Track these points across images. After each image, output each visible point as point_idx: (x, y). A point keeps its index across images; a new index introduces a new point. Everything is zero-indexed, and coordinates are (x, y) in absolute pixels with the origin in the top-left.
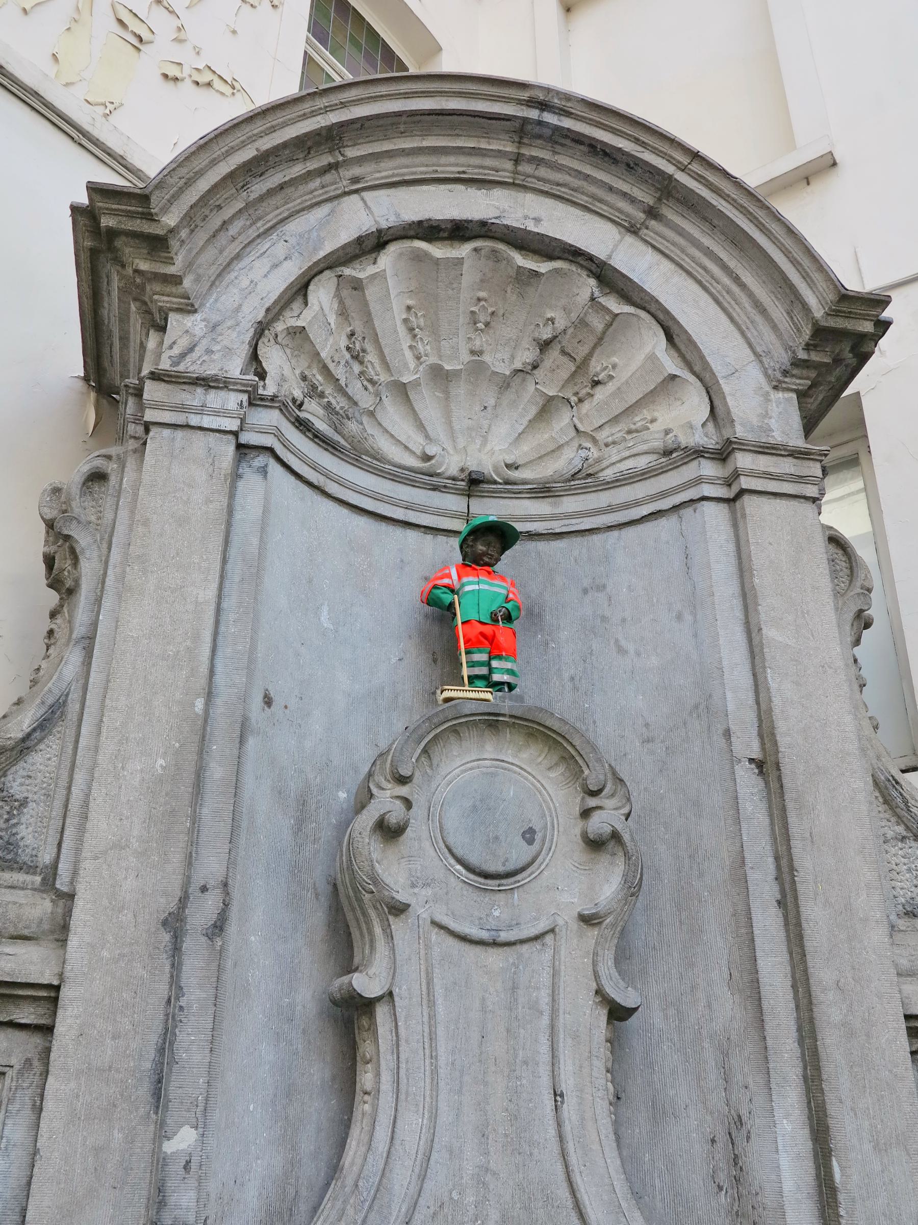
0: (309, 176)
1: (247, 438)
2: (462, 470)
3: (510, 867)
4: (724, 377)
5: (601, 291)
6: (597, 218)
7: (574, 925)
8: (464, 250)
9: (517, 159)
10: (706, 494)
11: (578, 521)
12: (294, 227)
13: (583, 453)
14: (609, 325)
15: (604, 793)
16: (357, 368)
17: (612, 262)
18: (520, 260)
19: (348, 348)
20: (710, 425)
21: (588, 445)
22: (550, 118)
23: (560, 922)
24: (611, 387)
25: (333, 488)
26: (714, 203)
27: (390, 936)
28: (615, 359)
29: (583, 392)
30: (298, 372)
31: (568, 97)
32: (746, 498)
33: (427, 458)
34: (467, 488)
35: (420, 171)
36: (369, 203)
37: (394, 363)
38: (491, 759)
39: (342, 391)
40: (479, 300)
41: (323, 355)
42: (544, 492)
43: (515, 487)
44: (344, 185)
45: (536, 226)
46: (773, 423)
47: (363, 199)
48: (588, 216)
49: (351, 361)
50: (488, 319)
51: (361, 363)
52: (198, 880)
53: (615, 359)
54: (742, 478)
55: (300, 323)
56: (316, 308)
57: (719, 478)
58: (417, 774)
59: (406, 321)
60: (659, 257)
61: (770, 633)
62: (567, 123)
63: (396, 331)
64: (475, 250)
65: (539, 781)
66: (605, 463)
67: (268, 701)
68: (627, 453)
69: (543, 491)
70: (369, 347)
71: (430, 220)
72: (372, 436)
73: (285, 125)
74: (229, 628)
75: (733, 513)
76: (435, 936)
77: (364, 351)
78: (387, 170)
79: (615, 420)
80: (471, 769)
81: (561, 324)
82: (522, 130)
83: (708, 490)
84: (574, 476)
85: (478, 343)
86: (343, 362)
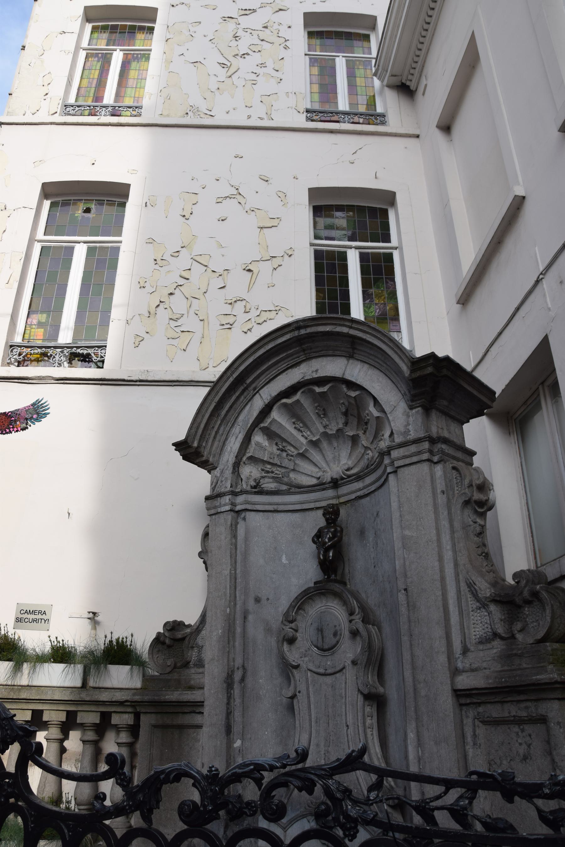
0: (238, 398)
1: (238, 508)
2: (332, 478)
3: (330, 646)
4: (390, 413)
5: (347, 389)
6: (338, 358)
7: (351, 665)
8: (298, 396)
9: (304, 350)
12: (241, 418)
14: (356, 401)
15: (356, 613)
16: (284, 454)
17: (344, 377)
18: (318, 390)
19: (278, 449)
21: (369, 452)
22: (303, 332)
23: (346, 664)
25: (281, 508)
26: (364, 337)
27: (294, 677)
28: (367, 412)
29: (364, 428)
30: (260, 469)
32: (399, 470)
33: (319, 478)
36: (262, 395)
37: (297, 445)
40: (316, 407)
41: (265, 459)
44: (252, 393)
45: (316, 374)
46: (410, 427)
47: (260, 395)
48: (335, 358)
49: (281, 453)
50: (323, 412)
51: (286, 451)
52: (236, 666)
53: (367, 412)
54: (395, 462)
55: (250, 454)
56: (254, 446)
58: (299, 618)
59: (295, 428)
60: (362, 364)
62: (309, 330)
63: (292, 434)
64: (302, 392)
66: (375, 458)
67: (258, 600)
70: (284, 444)
71: (281, 392)
72: (295, 479)
73: (221, 387)
74: (239, 580)
76: (309, 674)
77: (284, 447)
78: (263, 380)
83: (389, 470)
84: (367, 467)
85: (324, 423)
86: (276, 457)
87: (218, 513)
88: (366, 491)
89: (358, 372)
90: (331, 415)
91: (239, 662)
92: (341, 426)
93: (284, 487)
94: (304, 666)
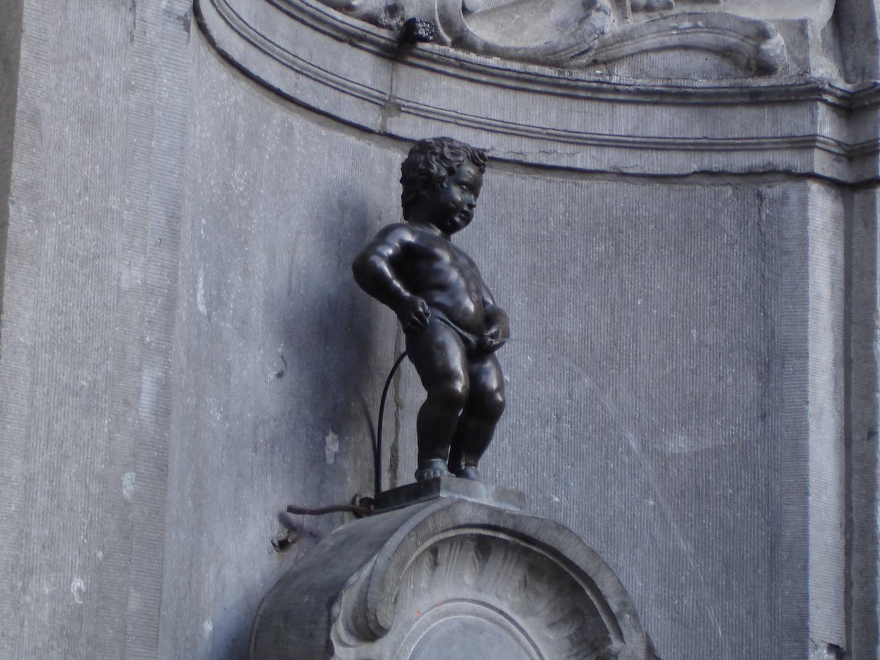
2: (393, 10)
10: (818, 170)
11: (570, 149)
13: (596, 18)
20: (829, 31)
34: (396, 45)
38: (473, 601)
42: (518, 79)
43: (473, 57)
57: (839, 144)
65: (534, 646)
66: (629, 47)
68: (675, 40)
75: (848, 208)
80: (447, 614)
83: (821, 163)
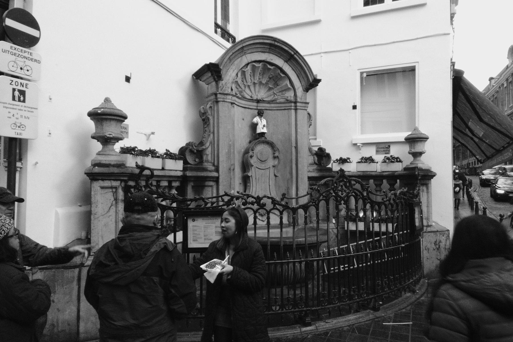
8: (260, 65)
9: (269, 49)
12: (236, 62)
18: (269, 66)
24: (280, 86)
31: (279, 40)
35: (255, 50)
39: (240, 87)
61: (299, 130)
62: (278, 44)
69: (269, 102)
76: (257, 169)
78: (249, 51)
79: (280, 92)
81: (274, 75)
82: (270, 45)
83: (293, 108)
87: (224, 101)
88: (270, 108)
89: (287, 68)
90: (265, 76)
91: (232, 162)
92: (266, 81)
93: (240, 96)
94: (255, 166)
